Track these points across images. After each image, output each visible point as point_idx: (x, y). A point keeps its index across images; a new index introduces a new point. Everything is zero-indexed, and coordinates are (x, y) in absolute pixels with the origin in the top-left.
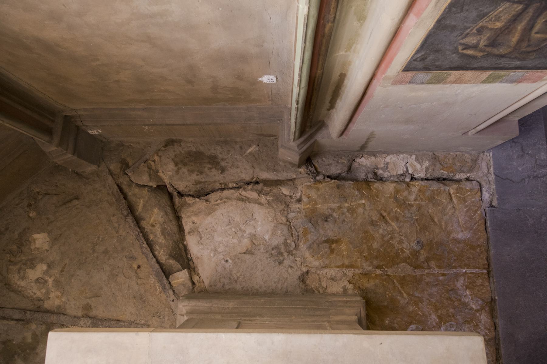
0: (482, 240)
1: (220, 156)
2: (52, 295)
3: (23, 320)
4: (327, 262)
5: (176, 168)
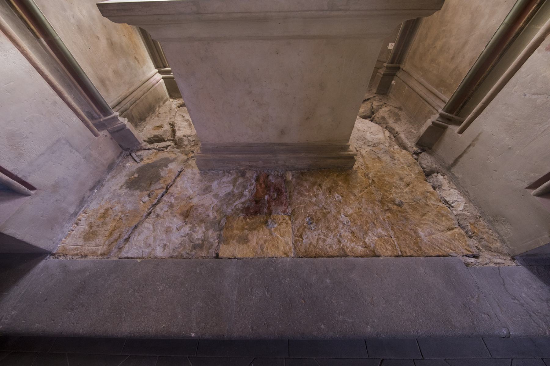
0: (426, 251)
4: (366, 156)
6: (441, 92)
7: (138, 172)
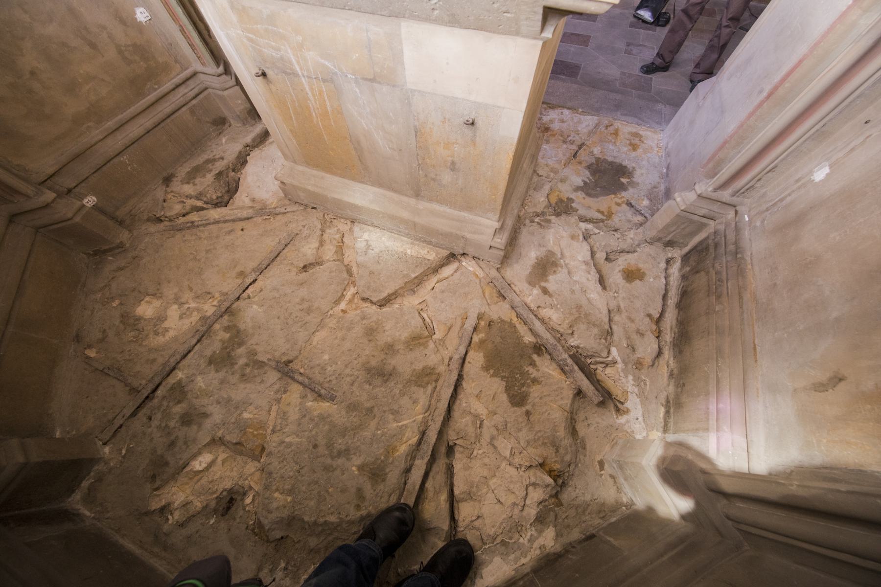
1: (211, 156)
3: (203, 336)
5: (191, 185)
6: (156, 90)
7: (623, 184)
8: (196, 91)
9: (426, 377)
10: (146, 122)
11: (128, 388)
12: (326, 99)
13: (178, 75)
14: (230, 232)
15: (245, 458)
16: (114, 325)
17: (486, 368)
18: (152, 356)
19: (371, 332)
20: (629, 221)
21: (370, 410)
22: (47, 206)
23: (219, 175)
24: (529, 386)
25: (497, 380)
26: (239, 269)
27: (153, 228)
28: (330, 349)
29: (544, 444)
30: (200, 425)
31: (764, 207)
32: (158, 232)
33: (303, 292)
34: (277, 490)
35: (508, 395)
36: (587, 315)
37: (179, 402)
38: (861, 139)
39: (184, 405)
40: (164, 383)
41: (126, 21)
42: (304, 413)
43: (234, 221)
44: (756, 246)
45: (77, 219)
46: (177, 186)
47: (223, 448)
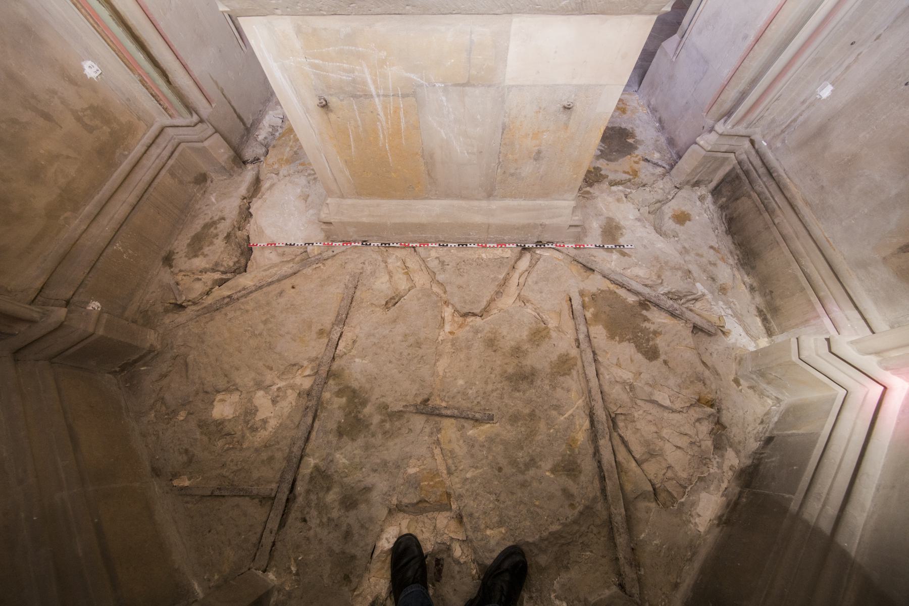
1: (208, 220)
2: (298, 380)
6: (126, 156)
8: (170, 148)
9: (564, 365)
10: (128, 197)
11: (257, 501)
12: (402, 115)
13: (145, 134)
14: (281, 294)
15: (430, 515)
16: (196, 440)
17: (612, 337)
18: (264, 456)
19: (491, 343)
20: (653, 174)
21: (532, 415)
22: (61, 326)
23: (228, 237)
24: (653, 339)
25: (625, 344)
26: (315, 328)
27: (181, 317)
28: (458, 373)
29: (692, 382)
30: (367, 501)
31: (778, 130)
32: (191, 319)
33: (401, 328)
34: (487, 527)
35: (641, 352)
36: (666, 263)
37: (329, 489)
38: (854, 56)
39: (336, 489)
40: (299, 477)
41: (77, 80)
42: (471, 443)
43: (279, 280)
44: (785, 163)
45: (101, 332)
46: (182, 262)
47: (401, 515)
